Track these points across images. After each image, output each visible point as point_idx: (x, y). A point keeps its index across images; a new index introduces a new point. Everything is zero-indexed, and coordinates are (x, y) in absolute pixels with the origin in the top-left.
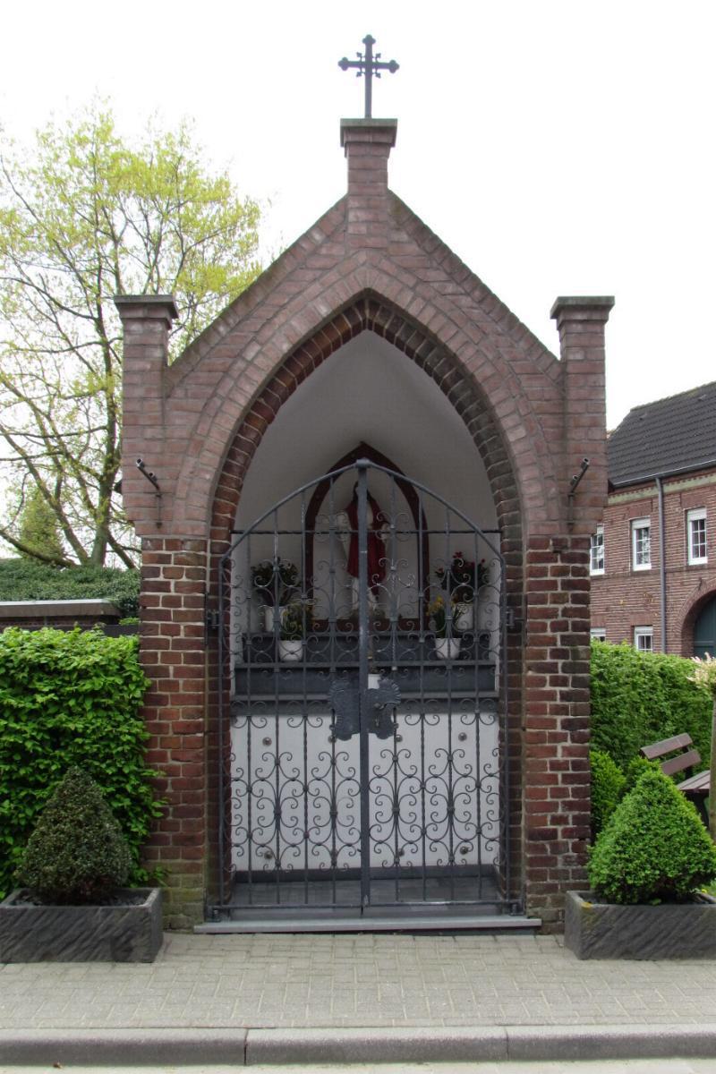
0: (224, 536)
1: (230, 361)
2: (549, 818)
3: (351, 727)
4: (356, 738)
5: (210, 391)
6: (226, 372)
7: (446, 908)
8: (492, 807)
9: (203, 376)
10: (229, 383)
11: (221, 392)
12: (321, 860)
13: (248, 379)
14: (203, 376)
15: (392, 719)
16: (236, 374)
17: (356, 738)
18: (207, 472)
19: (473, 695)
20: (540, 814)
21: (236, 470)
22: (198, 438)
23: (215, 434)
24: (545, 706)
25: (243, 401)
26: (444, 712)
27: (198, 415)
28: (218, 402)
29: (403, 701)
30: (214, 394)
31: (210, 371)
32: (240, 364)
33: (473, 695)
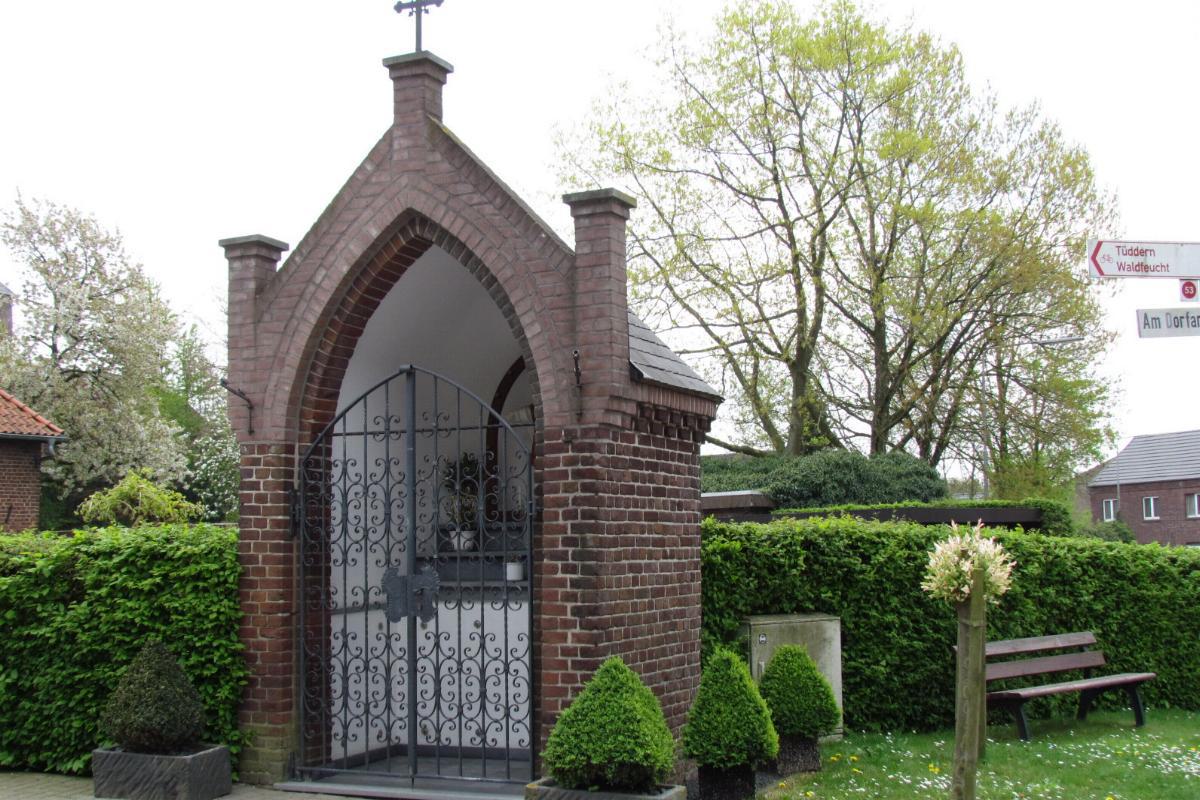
0: (308, 439)
1: (303, 286)
2: (560, 703)
3: (400, 610)
4: (404, 620)
5: (289, 313)
6: (301, 296)
7: (498, 786)
8: (524, 690)
9: (284, 302)
10: (303, 306)
11: (298, 314)
12: (469, 738)
13: (317, 299)
14: (284, 302)
15: (434, 605)
16: (308, 296)
17: (404, 620)
18: (287, 384)
19: (476, 584)
20: (552, 699)
21: (317, 380)
22: (280, 355)
23: (293, 352)
24: (557, 592)
25: (313, 320)
26: (478, 599)
27: (277, 337)
28: (295, 322)
29: (442, 588)
30: (292, 317)
31: (289, 296)
32: (312, 288)
33: (476, 584)
